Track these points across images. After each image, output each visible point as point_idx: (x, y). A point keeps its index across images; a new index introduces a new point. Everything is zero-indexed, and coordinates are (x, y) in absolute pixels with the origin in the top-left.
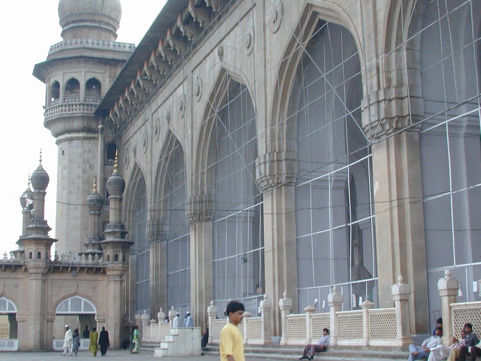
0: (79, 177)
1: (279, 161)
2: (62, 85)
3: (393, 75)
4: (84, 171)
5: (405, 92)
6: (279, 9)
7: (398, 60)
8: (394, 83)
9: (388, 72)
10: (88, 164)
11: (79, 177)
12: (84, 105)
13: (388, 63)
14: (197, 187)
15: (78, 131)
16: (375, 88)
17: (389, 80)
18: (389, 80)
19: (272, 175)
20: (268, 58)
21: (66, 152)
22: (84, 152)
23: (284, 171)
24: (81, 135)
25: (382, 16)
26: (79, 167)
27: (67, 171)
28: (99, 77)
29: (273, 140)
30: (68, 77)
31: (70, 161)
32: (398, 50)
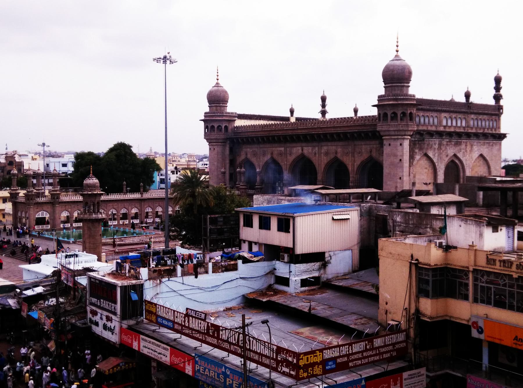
2: (216, 127)
10: (223, 153)
25: (355, 169)
28: (228, 125)
30: (218, 125)
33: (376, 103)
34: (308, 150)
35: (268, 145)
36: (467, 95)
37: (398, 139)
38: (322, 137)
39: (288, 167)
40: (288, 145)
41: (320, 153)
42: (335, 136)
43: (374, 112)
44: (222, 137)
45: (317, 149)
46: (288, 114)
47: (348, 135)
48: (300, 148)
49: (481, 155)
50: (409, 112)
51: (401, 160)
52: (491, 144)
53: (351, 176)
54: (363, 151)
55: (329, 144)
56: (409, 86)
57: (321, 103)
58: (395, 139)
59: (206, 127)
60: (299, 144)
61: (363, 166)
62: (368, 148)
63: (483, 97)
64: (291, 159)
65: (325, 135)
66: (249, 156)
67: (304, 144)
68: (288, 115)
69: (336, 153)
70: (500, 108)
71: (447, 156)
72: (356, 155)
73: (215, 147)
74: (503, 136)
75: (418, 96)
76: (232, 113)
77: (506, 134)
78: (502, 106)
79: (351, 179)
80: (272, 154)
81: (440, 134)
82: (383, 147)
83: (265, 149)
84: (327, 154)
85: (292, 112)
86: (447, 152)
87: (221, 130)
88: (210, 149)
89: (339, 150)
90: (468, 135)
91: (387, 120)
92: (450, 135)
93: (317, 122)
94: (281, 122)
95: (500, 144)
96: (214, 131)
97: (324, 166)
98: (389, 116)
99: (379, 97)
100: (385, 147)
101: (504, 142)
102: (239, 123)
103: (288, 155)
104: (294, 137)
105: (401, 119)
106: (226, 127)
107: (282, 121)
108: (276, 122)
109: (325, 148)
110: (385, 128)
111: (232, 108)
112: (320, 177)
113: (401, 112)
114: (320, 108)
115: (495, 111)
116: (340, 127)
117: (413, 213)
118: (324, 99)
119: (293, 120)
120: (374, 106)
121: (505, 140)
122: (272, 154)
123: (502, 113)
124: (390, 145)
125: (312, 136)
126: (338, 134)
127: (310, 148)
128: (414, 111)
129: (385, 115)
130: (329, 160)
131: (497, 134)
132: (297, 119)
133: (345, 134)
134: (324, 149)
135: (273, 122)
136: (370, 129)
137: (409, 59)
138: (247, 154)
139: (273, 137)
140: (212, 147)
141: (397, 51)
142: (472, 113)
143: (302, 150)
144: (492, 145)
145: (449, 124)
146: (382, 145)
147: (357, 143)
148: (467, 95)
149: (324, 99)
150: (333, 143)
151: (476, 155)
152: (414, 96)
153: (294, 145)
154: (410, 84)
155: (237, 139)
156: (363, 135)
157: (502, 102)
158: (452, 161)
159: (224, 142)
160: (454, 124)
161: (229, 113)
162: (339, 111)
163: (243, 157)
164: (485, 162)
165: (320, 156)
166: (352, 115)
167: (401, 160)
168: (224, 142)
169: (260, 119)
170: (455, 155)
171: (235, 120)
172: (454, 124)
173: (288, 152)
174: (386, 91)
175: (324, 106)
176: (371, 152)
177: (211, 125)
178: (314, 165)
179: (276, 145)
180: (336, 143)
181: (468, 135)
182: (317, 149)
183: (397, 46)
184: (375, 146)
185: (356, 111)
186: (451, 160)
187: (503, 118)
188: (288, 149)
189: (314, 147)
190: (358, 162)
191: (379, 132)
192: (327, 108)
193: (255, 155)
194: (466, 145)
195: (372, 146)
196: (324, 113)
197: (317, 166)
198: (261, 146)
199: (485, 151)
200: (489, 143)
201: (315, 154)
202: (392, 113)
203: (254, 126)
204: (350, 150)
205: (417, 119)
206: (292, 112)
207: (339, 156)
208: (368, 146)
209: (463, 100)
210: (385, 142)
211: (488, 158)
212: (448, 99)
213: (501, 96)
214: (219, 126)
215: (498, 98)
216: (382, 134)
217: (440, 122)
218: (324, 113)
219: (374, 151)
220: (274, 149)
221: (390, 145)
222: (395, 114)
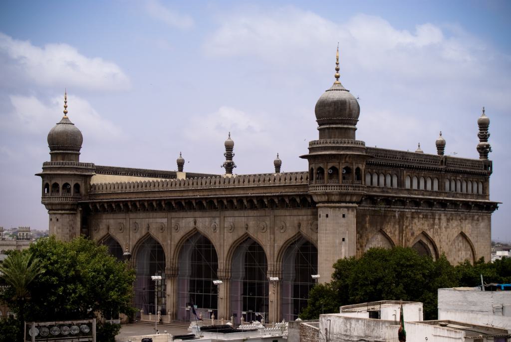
0: (67, 234)
1: (228, 272)
2: (61, 186)
3: (278, 268)
4: (70, 231)
5: (280, 273)
6: (233, 226)
7: (279, 264)
8: (278, 270)
9: (277, 266)
10: (72, 227)
11: (67, 234)
12: (73, 198)
13: (277, 264)
14: (173, 265)
15: (67, 210)
16: (273, 270)
17: (277, 269)
18: (277, 269)
19: (226, 276)
20: (225, 238)
21: (60, 220)
22: (70, 221)
23: (230, 275)
24: (68, 212)
26: (68, 228)
27: (60, 230)
28: (80, 183)
29: (226, 265)
30: (64, 182)
31: (62, 225)
32: (280, 262)
33: (307, 153)
34: (204, 223)
35: (142, 215)
36: (441, 146)
37: (340, 207)
38: (225, 202)
39: (173, 249)
40: (174, 214)
41: (222, 228)
42: (245, 202)
43: (304, 166)
44: (70, 201)
45: (217, 220)
46: (174, 168)
47: (265, 200)
48: (191, 220)
49: (463, 235)
50: (355, 167)
51: (343, 240)
52: (476, 217)
53: (269, 263)
54: (288, 225)
55: (236, 213)
56: (356, 129)
57: (225, 152)
58: (335, 207)
59: (45, 186)
60: (190, 214)
61: (288, 247)
62: (295, 220)
63: (463, 148)
64: (178, 236)
65: (230, 200)
66: (112, 232)
67: (198, 214)
68: (174, 168)
69: (247, 228)
70: (488, 165)
71: (413, 234)
72: (277, 232)
73: (58, 216)
74: (493, 206)
75: (369, 144)
76: (87, 164)
77: (497, 203)
78: (491, 162)
79: (269, 269)
80: (148, 228)
81: (402, 202)
82: (317, 220)
83: (138, 221)
84: (233, 228)
85: (181, 164)
86: (412, 229)
87: (69, 191)
88: (51, 220)
89: (252, 223)
90: (443, 204)
91: (323, 178)
92: (416, 203)
93: (217, 180)
94: (164, 180)
95: (489, 219)
96: (58, 191)
98: (325, 172)
99: (311, 144)
100: (320, 220)
101: (495, 215)
102: (98, 179)
103: (173, 230)
104: (183, 203)
105: (344, 178)
106: (77, 186)
107: (163, 177)
108: (155, 179)
110: (320, 190)
111: (86, 156)
112: (222, 263)
113: (344, 167)
114: (224, 160)
115: (479, 171)
116: (253, 188)
117: (358, 320)
118: (229, 147)
119: (181, 176)
120: (303, 157)
121: (496, 212)
122: (148, 228)
123: (490, 173)
124: (327, 216)
125: (210, 201)
126: (250, 199)
127: (207, 219)
128: (362, 167)
129: (321, 171)
130: (236, 238)
131: (485, 203)
132: (189, 175)
133: (260, 199)
134: (229, 221)
135: (151, 179)
136: (301, 191)
137: (354, 90)
138: (108, 228)
139: (150, 202)
140: (54, 217)
141: (337, 77)
142: (447, 171)
143: (195, 223)
144: (478, 220)
145: (415, 186)
146: (315, 216)
147: (278, 212)
148: (441, 146)
149: (229, 147)
150: (242, 213)
151: (455, 232)
152: (363, 143)
153: (182, 214)
154: (357, 126)
155: (94, 204)
156: (287, 200)
157: (491, 157)
158: (420, 242)
160: (422, 187)
161: (82, 164)
162: (252, 164)
163: (102, 233)
164: (467, 244)
165: (223, 232)
166: (272, 170)
167: (343, 240)
168: (73, 209)
169: (131, 175)
170: (424, 234)
171: (92, 175)
172: (422, 187)
173: (173, 226)
174: (321, 136)
175: (229, 156)
177: (53, 182)
178: (213, 247)
179: (155, 214)
180: (246, 213)
181: (443, 204)
182: (217, 220)
183: (337, 70)
184: (305, 218)
185: (278, 165)
186: (418, 240)
187: (492, 179)
188: (173, 221)
189: (214, 217)
190: (280, 243)
191: (311, 196)
192: (234, 159)
193: (122, 229)
194: (440, 219)
195: (301, 217)
196: (229, 167)
197: (217, 248)
198: (132, 215)
199: (467, 228)
200: (473, 216)
201: (215, 229)
202: (330, 169)
203: (121, 185)
204: (268, 223)
205: (368, 178)
206: (181, 164)
207: (251, 232)
208: (295, 218)
209: (434, 152)
210: (321, 212)
211: (470, 238)
212: (413, 150)
213: (488, 146)
214: (66, 186)
215: (484, 150)
216: (316, 199)
217: (401, 184)
218: (229, 167)
219: (304, 225)
220: (151, 220)
221: (327, 216)
222: (335, 170)
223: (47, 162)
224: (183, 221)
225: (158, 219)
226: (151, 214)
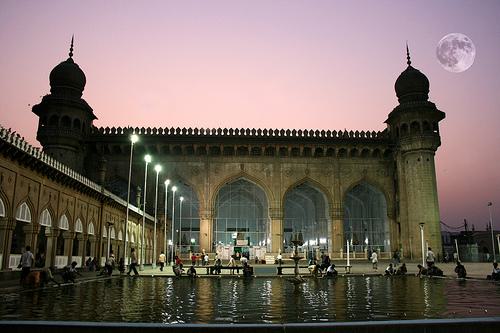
45: (271, 166)
62: (361, 167)
69: (308, 172)
84: (291, 172)
97: (285, 189)
109: (289, 165)
143: (242, 168)
159: (77, 148)
176: (365, 171)
177: (63, 115)
182: (271, 166)
184: (370, 166)
188: (212, 166)
189: (267, 164)
207: (313, 177)
214: (77, 121)
223: (48, 96)
224: (227, 165)
225: (190, 163)
226: (182, 158)
